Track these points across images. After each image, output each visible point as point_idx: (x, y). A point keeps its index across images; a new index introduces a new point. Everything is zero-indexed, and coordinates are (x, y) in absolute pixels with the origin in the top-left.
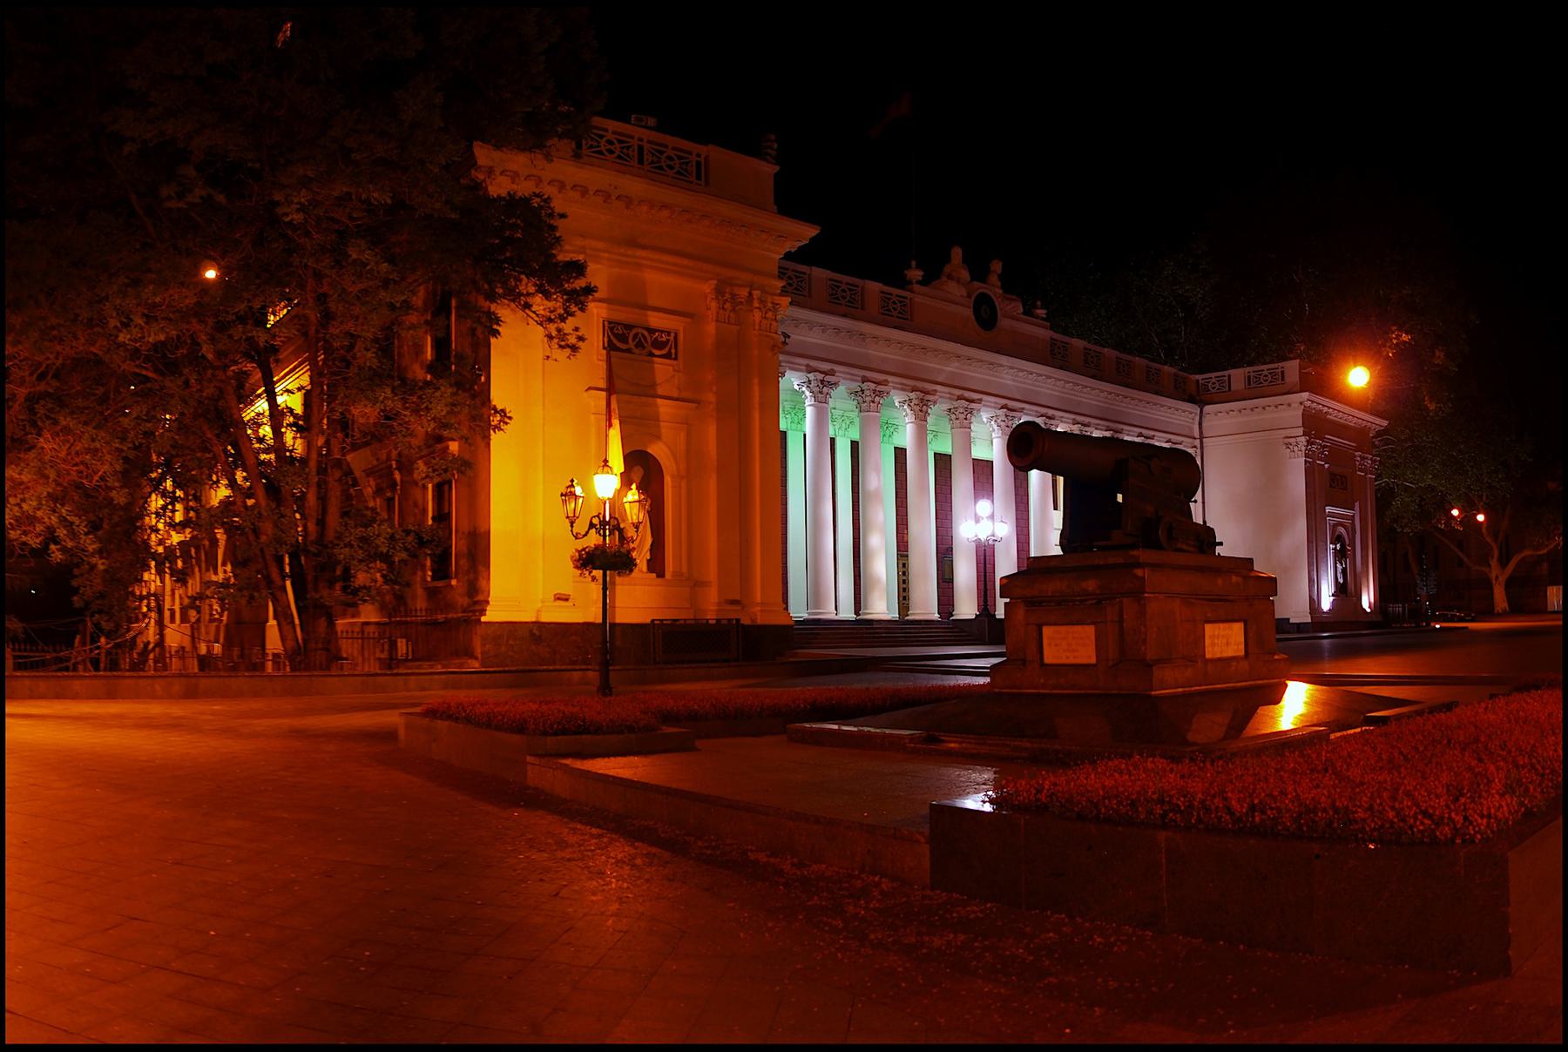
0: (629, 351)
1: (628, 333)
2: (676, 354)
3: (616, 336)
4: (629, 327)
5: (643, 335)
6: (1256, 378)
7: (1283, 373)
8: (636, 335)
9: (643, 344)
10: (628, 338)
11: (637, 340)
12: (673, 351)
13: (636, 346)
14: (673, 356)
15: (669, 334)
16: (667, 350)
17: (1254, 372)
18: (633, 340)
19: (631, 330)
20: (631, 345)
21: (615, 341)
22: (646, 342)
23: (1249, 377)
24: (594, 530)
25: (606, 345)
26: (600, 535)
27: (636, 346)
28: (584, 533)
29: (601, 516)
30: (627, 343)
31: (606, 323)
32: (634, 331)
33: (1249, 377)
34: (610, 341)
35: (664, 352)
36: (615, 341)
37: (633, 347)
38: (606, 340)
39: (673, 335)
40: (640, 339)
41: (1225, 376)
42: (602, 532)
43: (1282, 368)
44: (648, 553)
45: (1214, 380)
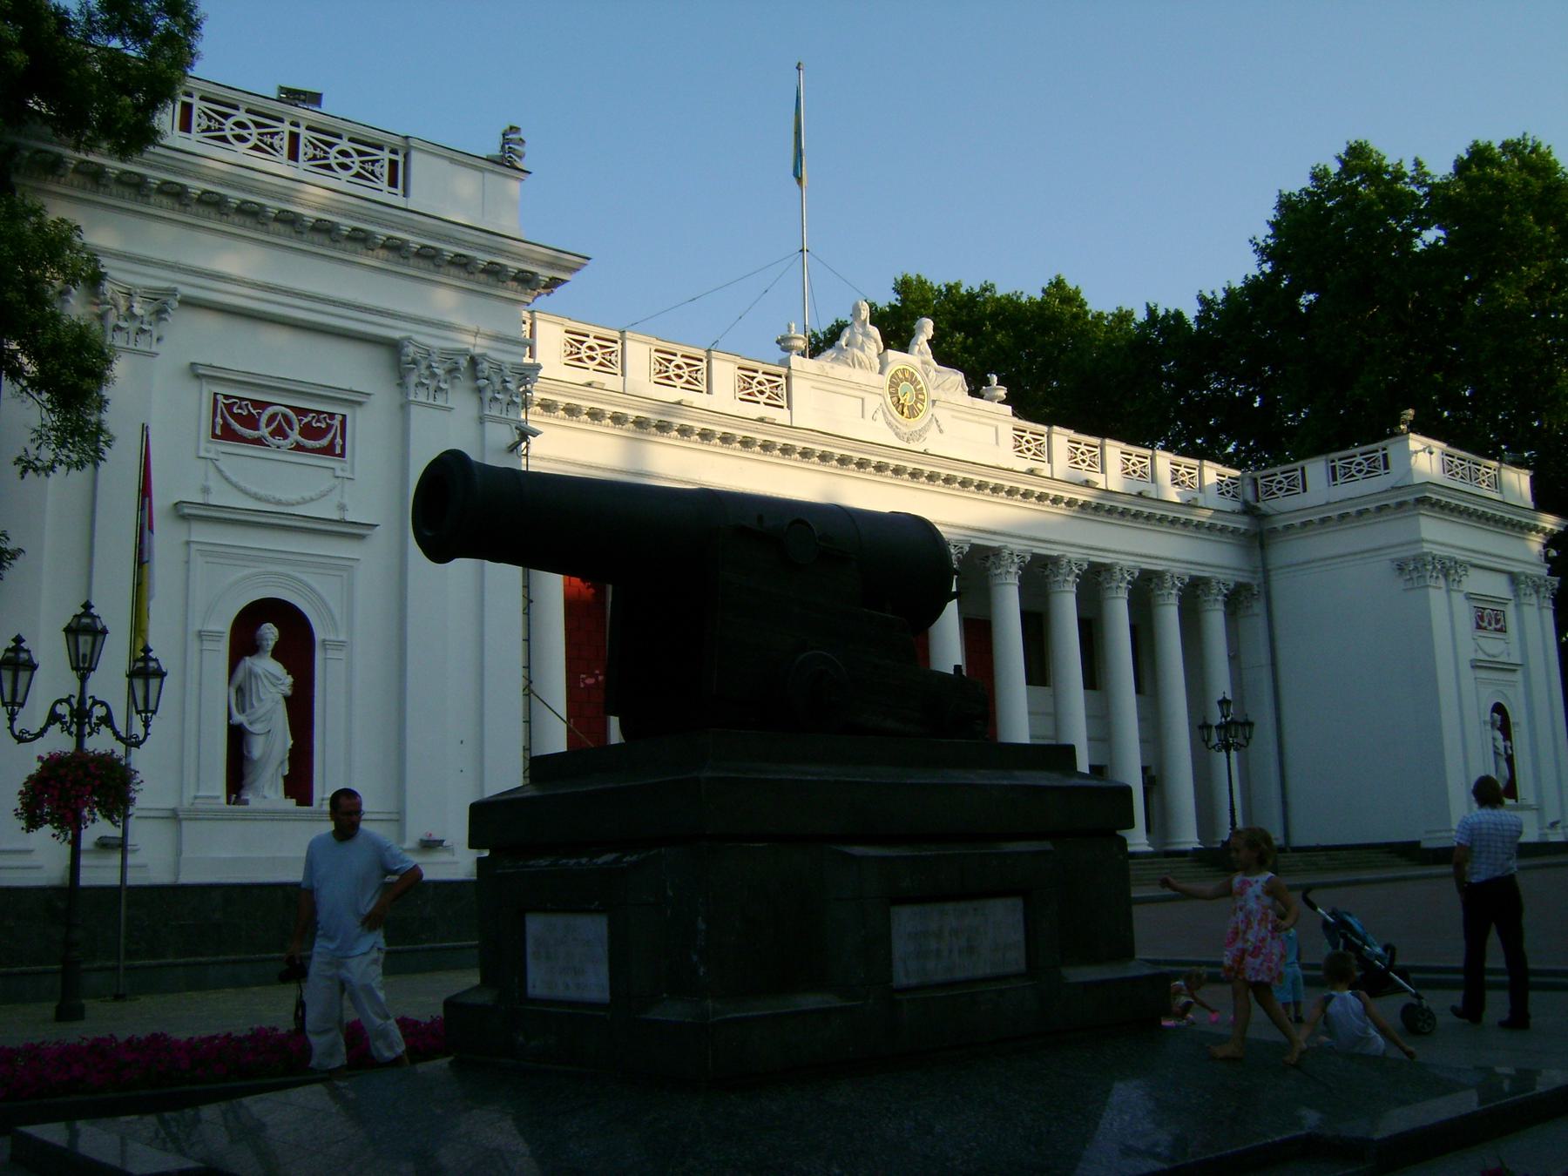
0: (259, 441)
1: (259, 414)
2: (343, 447)
3: (238, 417)
4: (266, 405)
5: (285, 417)
6: (1344, 468)
7: (1385, 456)
8: (272, 418)
9: (284, 431)
10: (258, 420)
11: (276, 423)
12: (339, 440)
13: (273, 434)
14: (338, 451)
15: (332, 416)
16: (330, 436)
17: (1340, 460)
18: (268, 425)
19: (264, 410)
20: (264, 431)
21: (237, 426)
22: (292, 430)
23: (1334, 468)
24: (58, 725)
25: (218, 432)
26: (70, 733)
27: (273, 434)
28: (37, 730)
29: (74, 701)
30: (256, 428)
31: (220, 398)
32: (271, 410)
33: (1334, 468)
34: (226, 426)
35: (325, 442)
36: (237, 426)
37: (267, 435)
38: (219, 420)
39: (339, 418)
40: (280, 421)
41: (1296, 470)
42: (74, 728)
43: (1384, 449)
44: (287, 763)
45: (1279, 478)
